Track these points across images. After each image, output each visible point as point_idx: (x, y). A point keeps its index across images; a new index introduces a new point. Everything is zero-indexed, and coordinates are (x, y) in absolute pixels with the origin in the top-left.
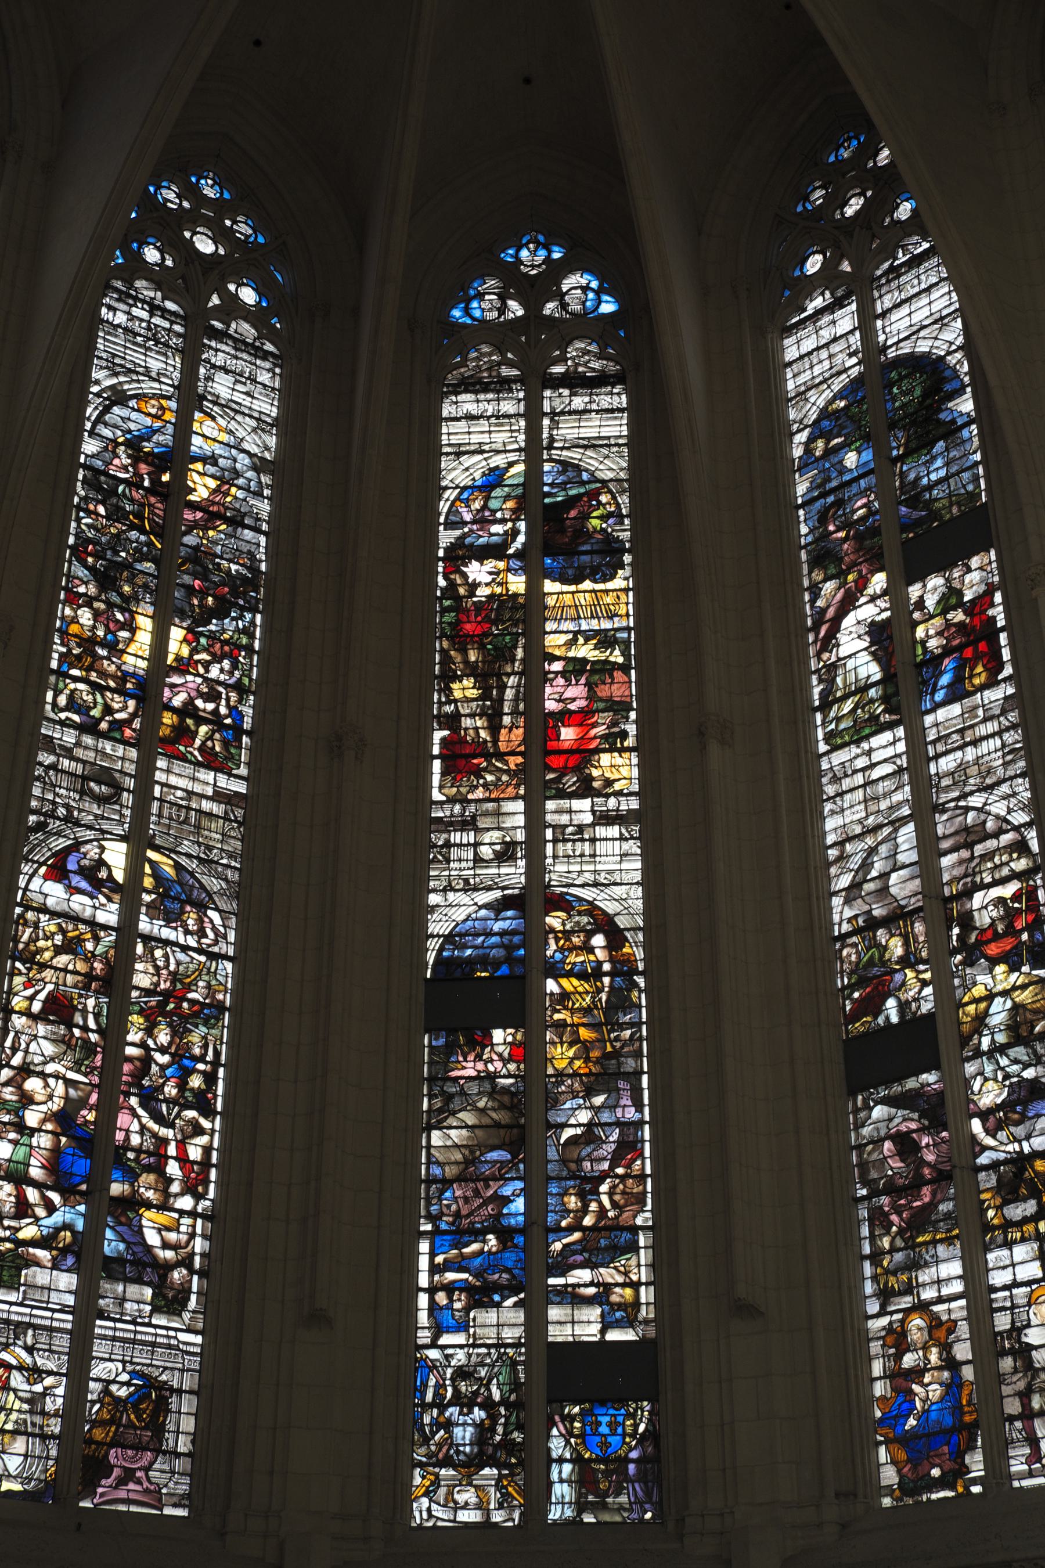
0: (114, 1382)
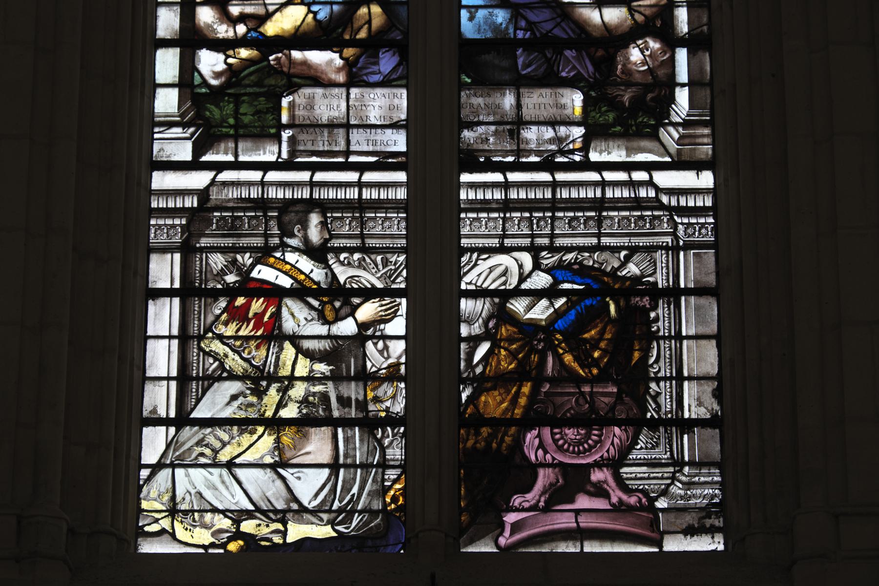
0: (517, 292)
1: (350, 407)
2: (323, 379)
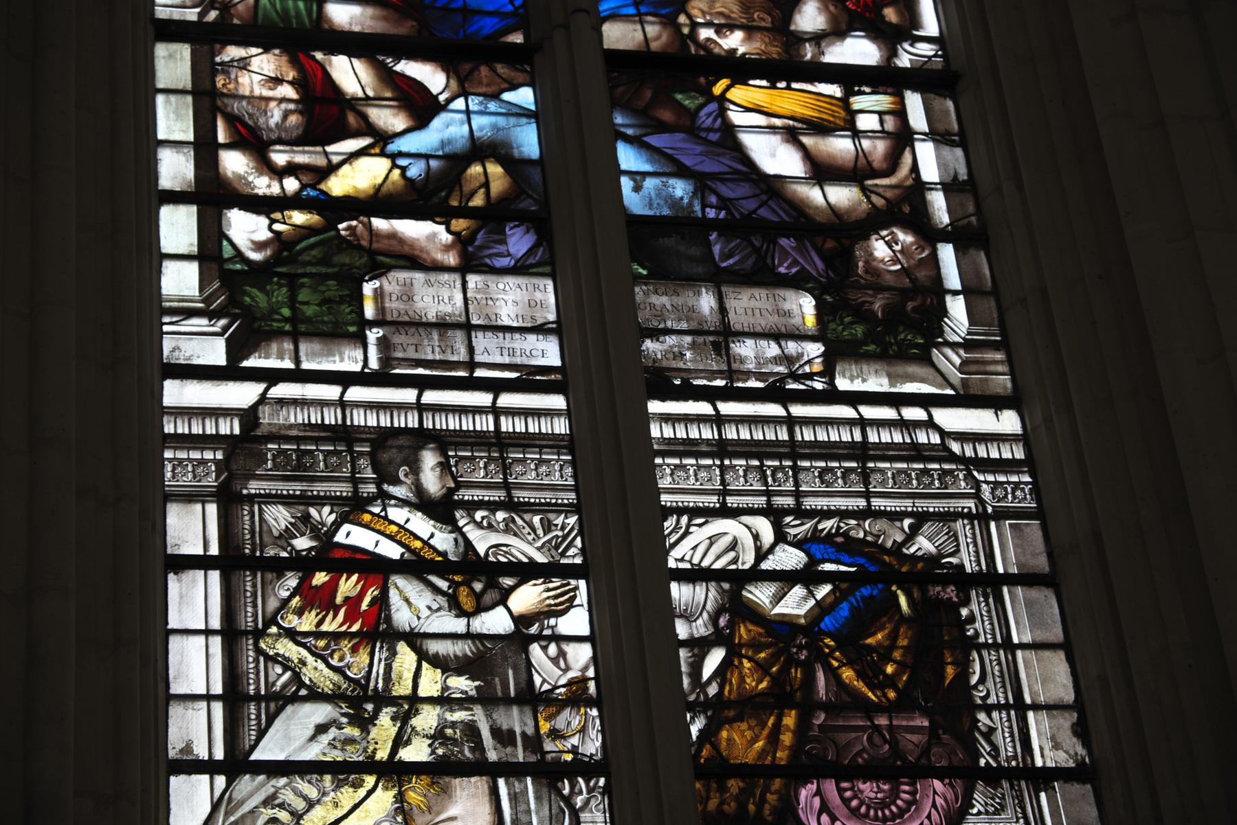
0: (756, 575)
1: (515, 745)
2: (465, 702)
